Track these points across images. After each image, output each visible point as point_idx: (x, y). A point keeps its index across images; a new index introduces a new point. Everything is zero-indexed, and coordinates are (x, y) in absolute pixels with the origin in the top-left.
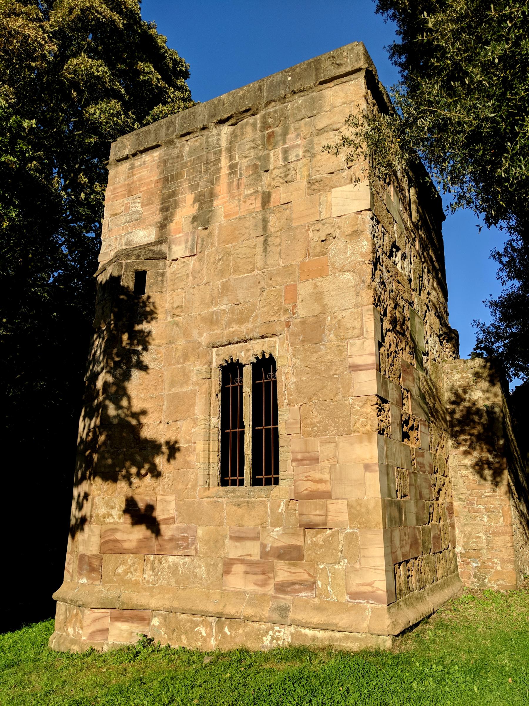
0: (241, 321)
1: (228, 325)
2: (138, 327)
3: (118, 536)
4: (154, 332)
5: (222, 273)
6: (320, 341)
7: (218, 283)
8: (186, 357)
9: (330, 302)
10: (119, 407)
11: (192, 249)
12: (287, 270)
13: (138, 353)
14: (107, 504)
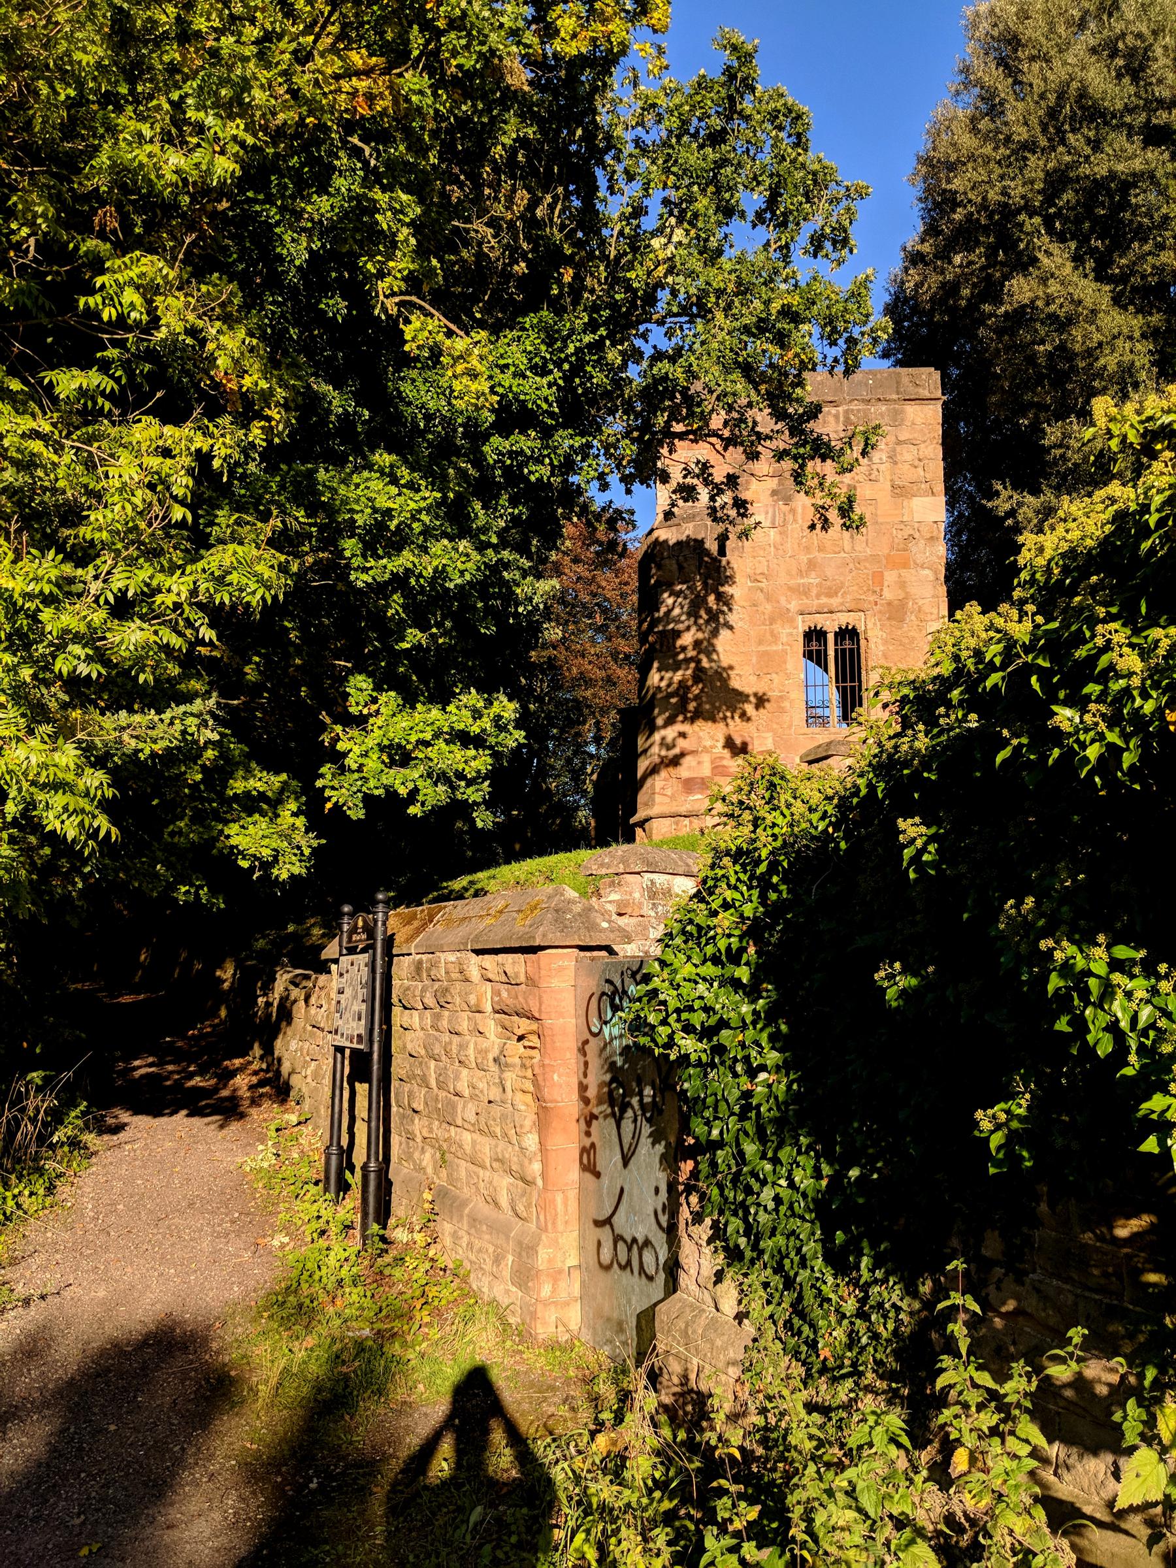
0: (829, 595)
1: (818, 596)
2: (721, 589)
3: (725, 763)
4: (736, 596)
5: (808, 549)
6: (902, 621)
7: (804, 558)
8: (772, 621)
9: (913, 590)
10: (711, 660)
11: (773, 522)
12: (875, 558)
13: (723, 612)
14: (712, 738)
